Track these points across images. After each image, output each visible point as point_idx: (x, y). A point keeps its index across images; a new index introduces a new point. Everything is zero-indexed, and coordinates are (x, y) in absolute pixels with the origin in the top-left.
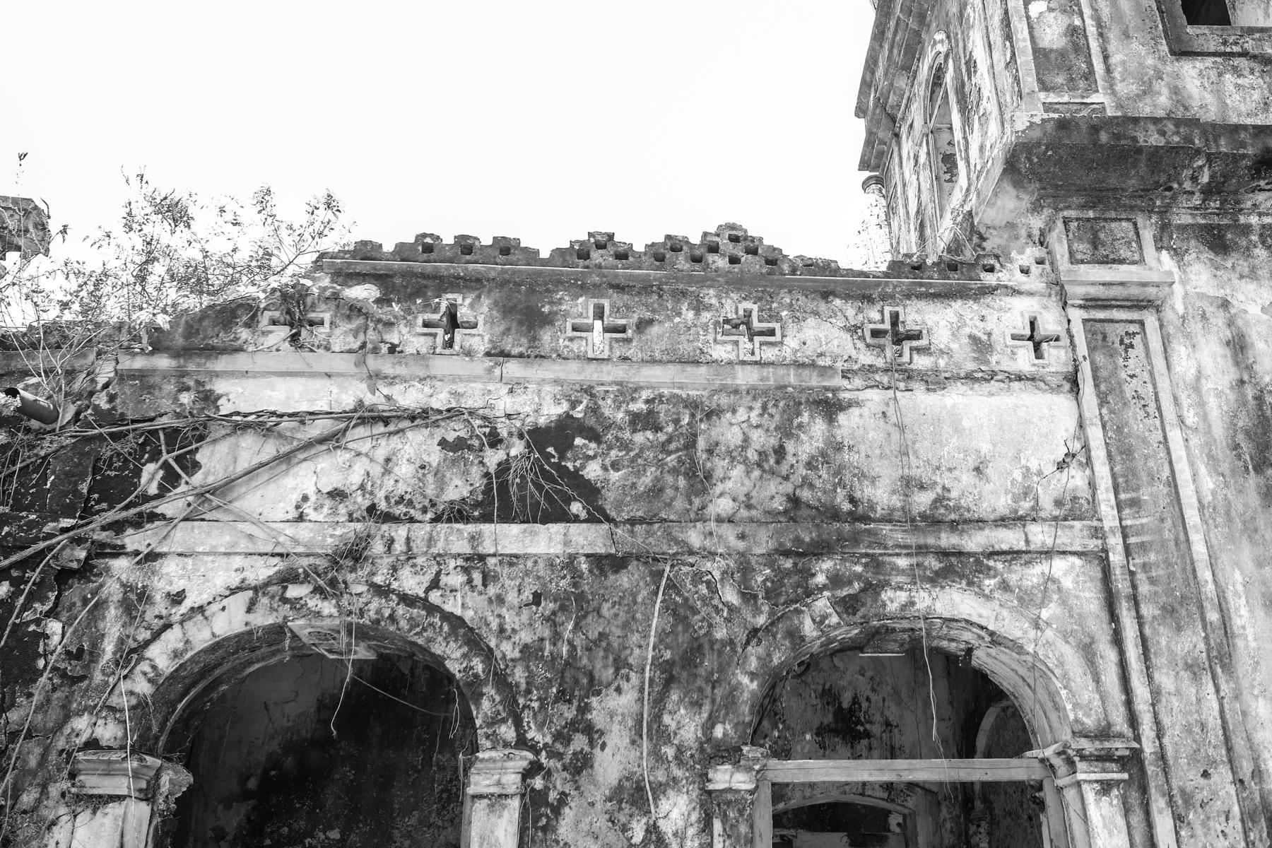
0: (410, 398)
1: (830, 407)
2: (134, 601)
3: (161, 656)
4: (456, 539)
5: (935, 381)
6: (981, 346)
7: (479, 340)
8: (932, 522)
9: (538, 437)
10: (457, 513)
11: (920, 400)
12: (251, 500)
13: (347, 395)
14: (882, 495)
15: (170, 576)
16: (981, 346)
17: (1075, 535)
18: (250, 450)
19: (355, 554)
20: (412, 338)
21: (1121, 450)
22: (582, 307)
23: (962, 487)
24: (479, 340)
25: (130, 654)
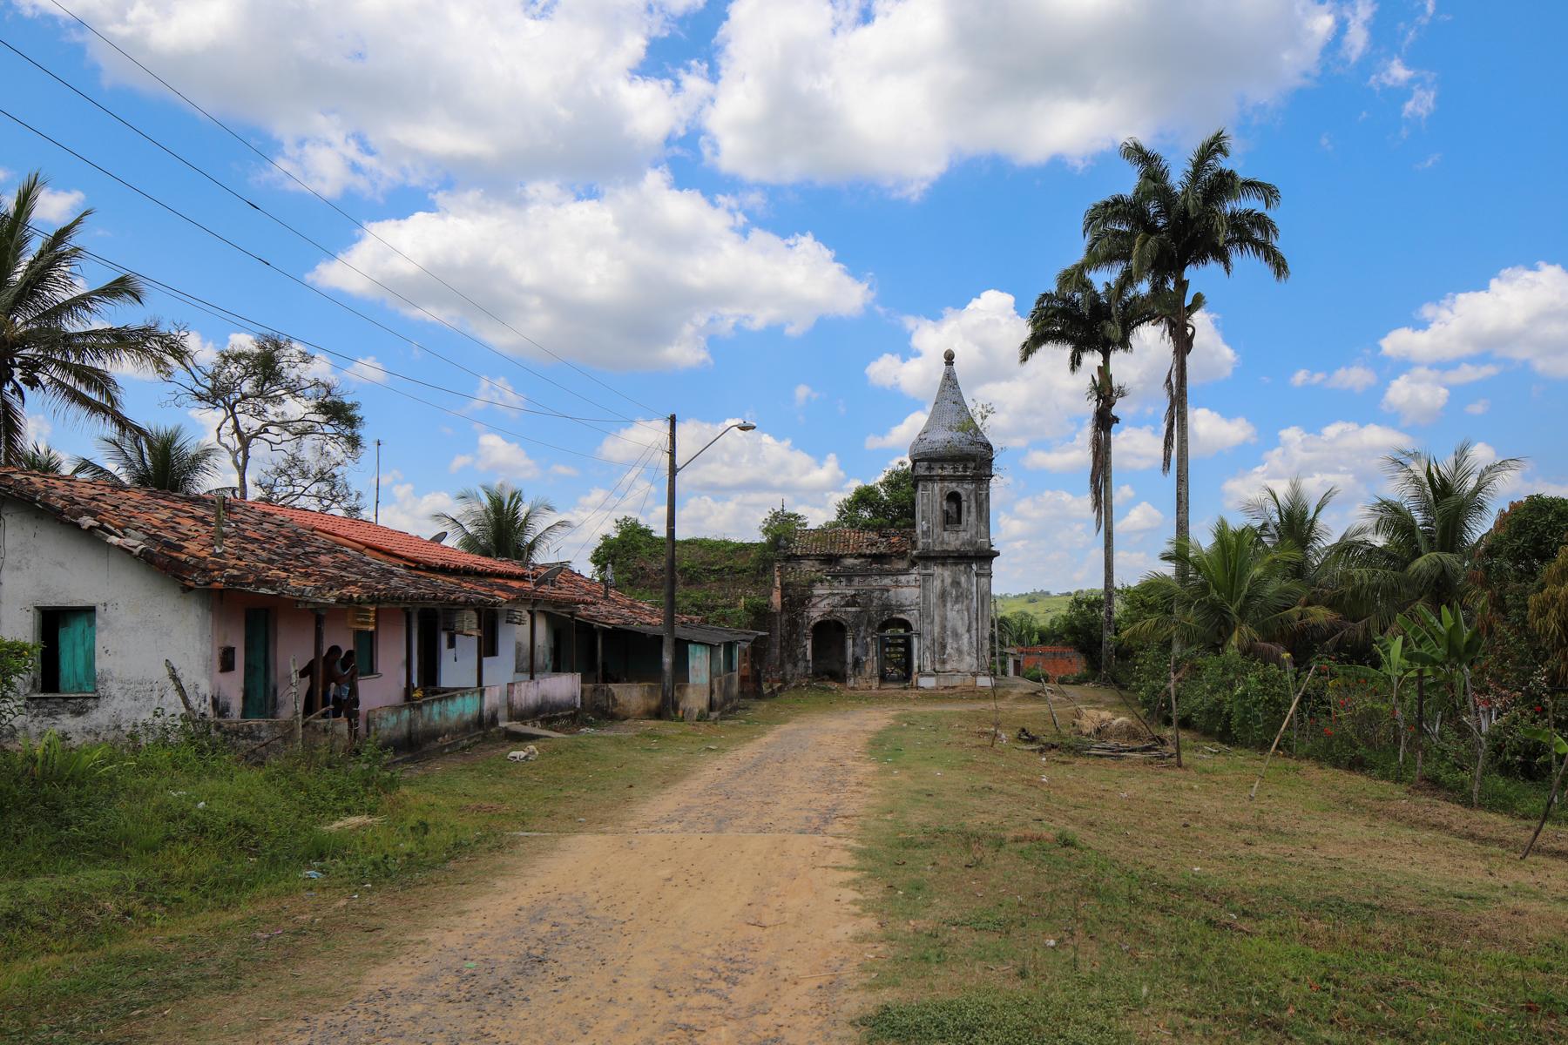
0: (836, 592)
1: (888, 591)
2: (808, 617)
3: (812, 623)
4: (843, 609)
5: (902, 587)
6: (908, 582)
7: (844, 584)
8: (900, 606)
9: (852, 596)
10: (843, 606)
11: (899, 590)
12: (819, 605)
13: (829, 591)
14: (894, 602)
15: (811, 614)
16: (908, 582)
17: (917, 607)
18: (818, 599)
19: (832, 611)
20: (836, 584)
21: (924, 596)
22: (857, 579)
23: (904, 601)
24: (844, 584)
25: (808, 623)
